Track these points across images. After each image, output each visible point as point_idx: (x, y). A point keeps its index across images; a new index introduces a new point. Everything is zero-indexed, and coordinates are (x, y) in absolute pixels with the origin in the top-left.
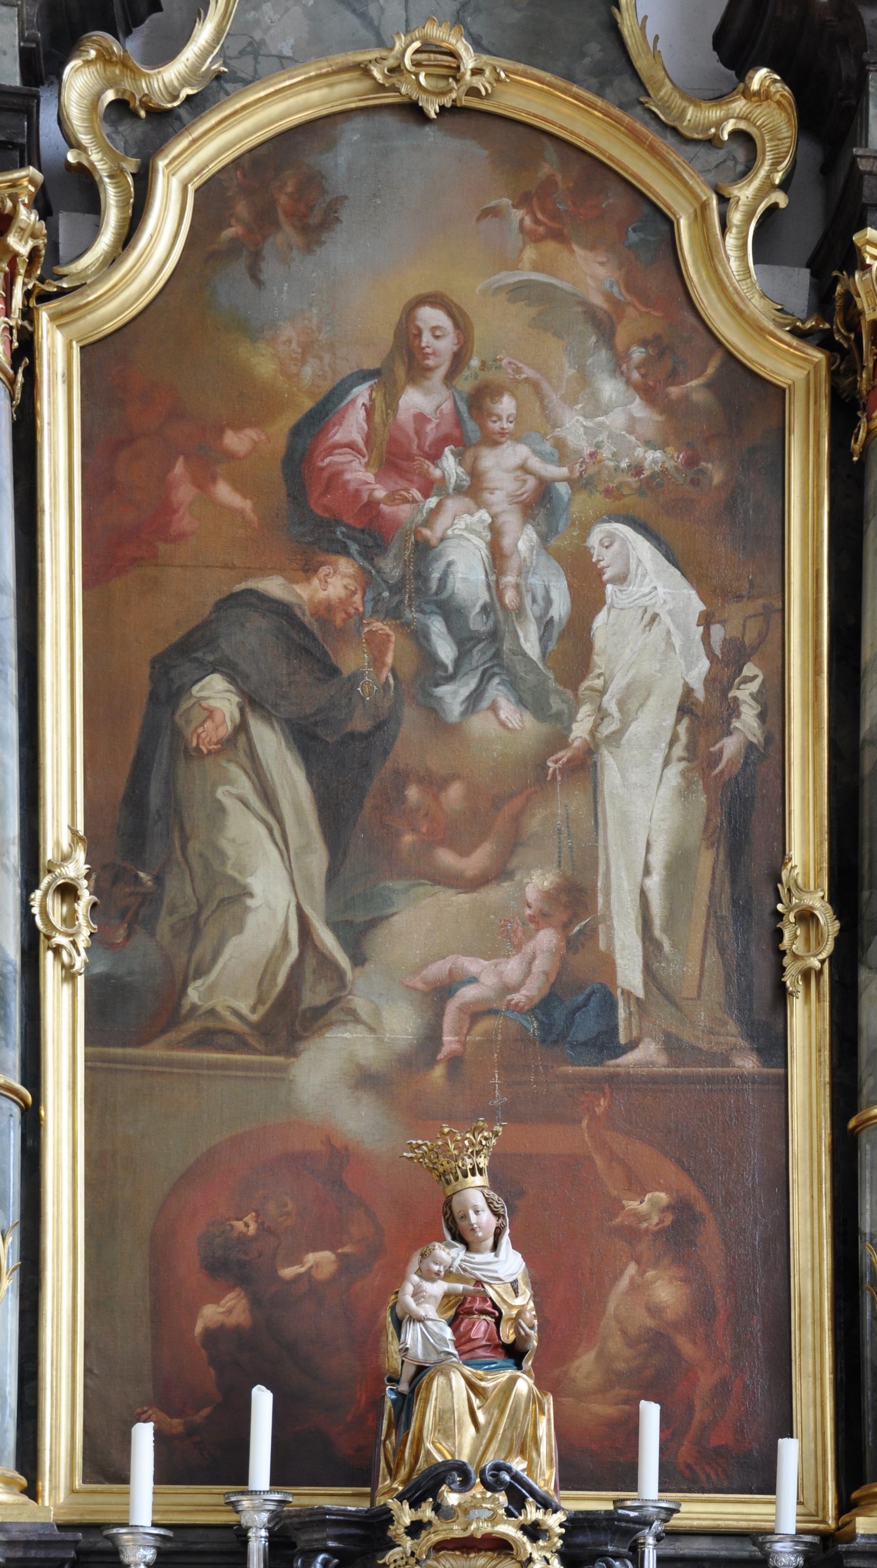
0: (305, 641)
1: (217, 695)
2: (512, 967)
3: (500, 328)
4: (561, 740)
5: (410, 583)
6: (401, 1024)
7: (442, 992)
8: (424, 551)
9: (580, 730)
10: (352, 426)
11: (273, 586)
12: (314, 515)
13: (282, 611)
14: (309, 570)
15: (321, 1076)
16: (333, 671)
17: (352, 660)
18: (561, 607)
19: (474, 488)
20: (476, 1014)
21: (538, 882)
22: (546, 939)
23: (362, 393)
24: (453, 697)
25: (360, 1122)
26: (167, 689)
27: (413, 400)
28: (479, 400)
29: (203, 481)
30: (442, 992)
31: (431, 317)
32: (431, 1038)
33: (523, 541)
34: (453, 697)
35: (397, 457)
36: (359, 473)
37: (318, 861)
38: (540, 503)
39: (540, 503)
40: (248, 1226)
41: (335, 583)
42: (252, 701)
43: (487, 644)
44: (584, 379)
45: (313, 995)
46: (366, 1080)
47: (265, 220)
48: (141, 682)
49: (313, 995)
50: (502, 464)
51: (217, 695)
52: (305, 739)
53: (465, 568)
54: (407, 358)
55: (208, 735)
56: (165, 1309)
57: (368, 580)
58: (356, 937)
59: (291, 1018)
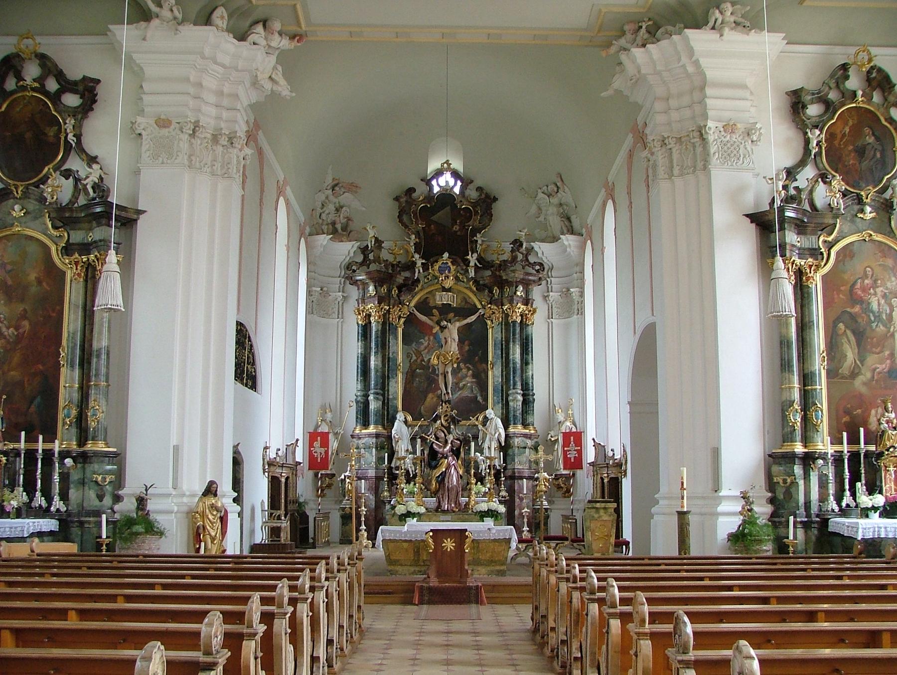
0: (853, 317)
1: (841, 326)
2: (884, 366)
3: (878, 270)
4: (889, 331)
5: (867, 309)
6: (869, 375)
7: (874, 370)
8: (869, 304)
9: (892, 330)
10: (858, 286)
11: (848, 310)
12: (854, 299)
13: (850, 313)
14: (853, 307)
15: (858, 382)
16: (857, 322)
17: (860, 320)
18: (888, 312)
19: (875, 294)
20: (879, 373)
21: (887, 353)
22: (888, 361)
23: (859, 281)
24: (874, 325)
25: (864, 390)
26: (835, 326)
27: (866, 281)
28: (875, 281)
29: (838, 295)
30: (874, 370)
31: (868, 269)
32: (873, 377)
33: (883, 302)
34: (874, 325)
35: (865, 290)
36: (859, 292)
37: (856, 351)
38: (884, 296)
39: (884, 296)
40: (849, 406)
41: (857, 309)
42: (846, 327)
43: (878, 317)
44: (890, 278)
45: (856, 371)
46: (864, 384)
47: (845, 256)
48: (831, 325)
49: (856, 371)
50: (879, 290)
51: (841, 326)
52: (854, 332)
53: (875, 306)
54: (865, 276)
55: (841, 332)
56: (838, 419)
57: (861, 308)
58: (862, 362)
59: (854, 375)
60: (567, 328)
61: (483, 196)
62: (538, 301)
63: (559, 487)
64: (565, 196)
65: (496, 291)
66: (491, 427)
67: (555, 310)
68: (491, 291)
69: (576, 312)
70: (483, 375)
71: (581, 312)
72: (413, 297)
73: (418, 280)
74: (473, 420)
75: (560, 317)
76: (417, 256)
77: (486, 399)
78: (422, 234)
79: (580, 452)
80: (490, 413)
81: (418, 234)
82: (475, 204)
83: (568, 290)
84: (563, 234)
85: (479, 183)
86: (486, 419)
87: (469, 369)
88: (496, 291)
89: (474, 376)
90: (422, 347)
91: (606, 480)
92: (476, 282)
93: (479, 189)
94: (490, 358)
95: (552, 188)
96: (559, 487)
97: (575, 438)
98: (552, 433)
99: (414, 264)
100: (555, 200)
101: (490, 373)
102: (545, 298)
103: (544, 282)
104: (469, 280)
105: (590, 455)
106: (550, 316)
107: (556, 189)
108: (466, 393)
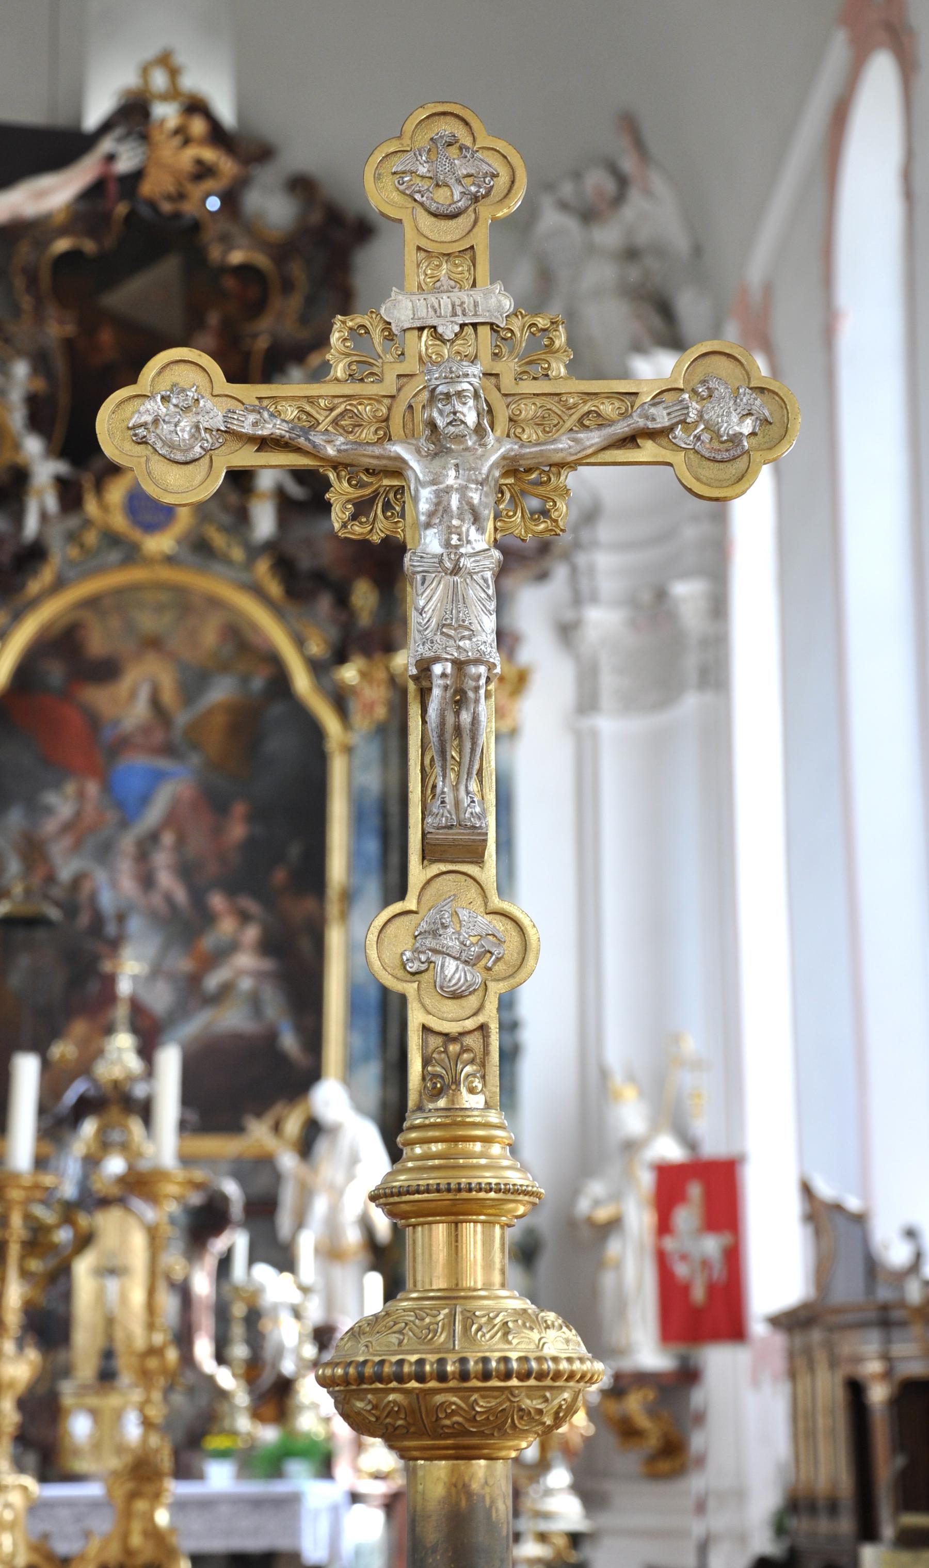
60: (656, 752)
61: (316, 217)
62: (538, 649)
63: (628, 1431)
64: (654, 213)
65: (364, 596)
66: (329, 1165)
67: (608, 681)
68: (342, 600)
69: (692, 674)
70: (305, 945)
71: (715, 675)
72: (17, 617)
73: (35, 554)
74: (259, 1133)
75: (630, 704)
76: (33, 446)
77: (314, 1040)
78: (60, 365)
79: (734, 1258)
80: (331, 1099)
81: (41, 362)
82: (283, 250)
83: (661, 595)
84: (639, 348)
85: (298, 156)
86: (313, 1132)
87: (244, 918)
88: (364, 596)
89: (269, 946)
90: (50, 826)
91: (878, 1394)
92: (285, 566)
93: (302, 186)
94: (338, 867)
95: (597, 181)
96: (628, 1431)
97: (708, 1187)
98: (596, 1188)
99: (20, 477)
100: (609, 235)
101: (335, 938)
102: (567, 632)
103: (561, 573)
104: (254, 552)
105: (778, 1274)
106: (587, 702)
107: (610, 186)
108: (232, 1019)
